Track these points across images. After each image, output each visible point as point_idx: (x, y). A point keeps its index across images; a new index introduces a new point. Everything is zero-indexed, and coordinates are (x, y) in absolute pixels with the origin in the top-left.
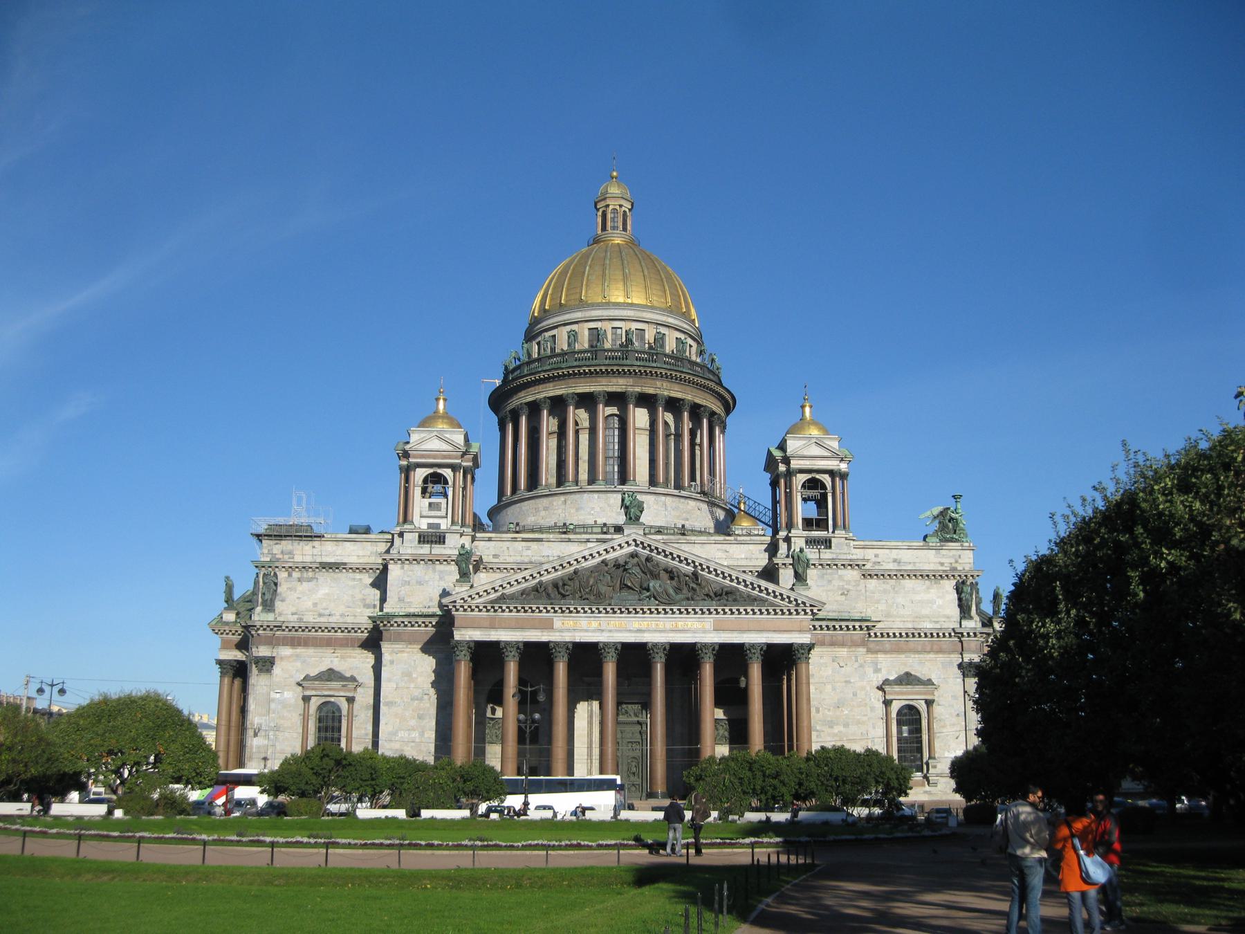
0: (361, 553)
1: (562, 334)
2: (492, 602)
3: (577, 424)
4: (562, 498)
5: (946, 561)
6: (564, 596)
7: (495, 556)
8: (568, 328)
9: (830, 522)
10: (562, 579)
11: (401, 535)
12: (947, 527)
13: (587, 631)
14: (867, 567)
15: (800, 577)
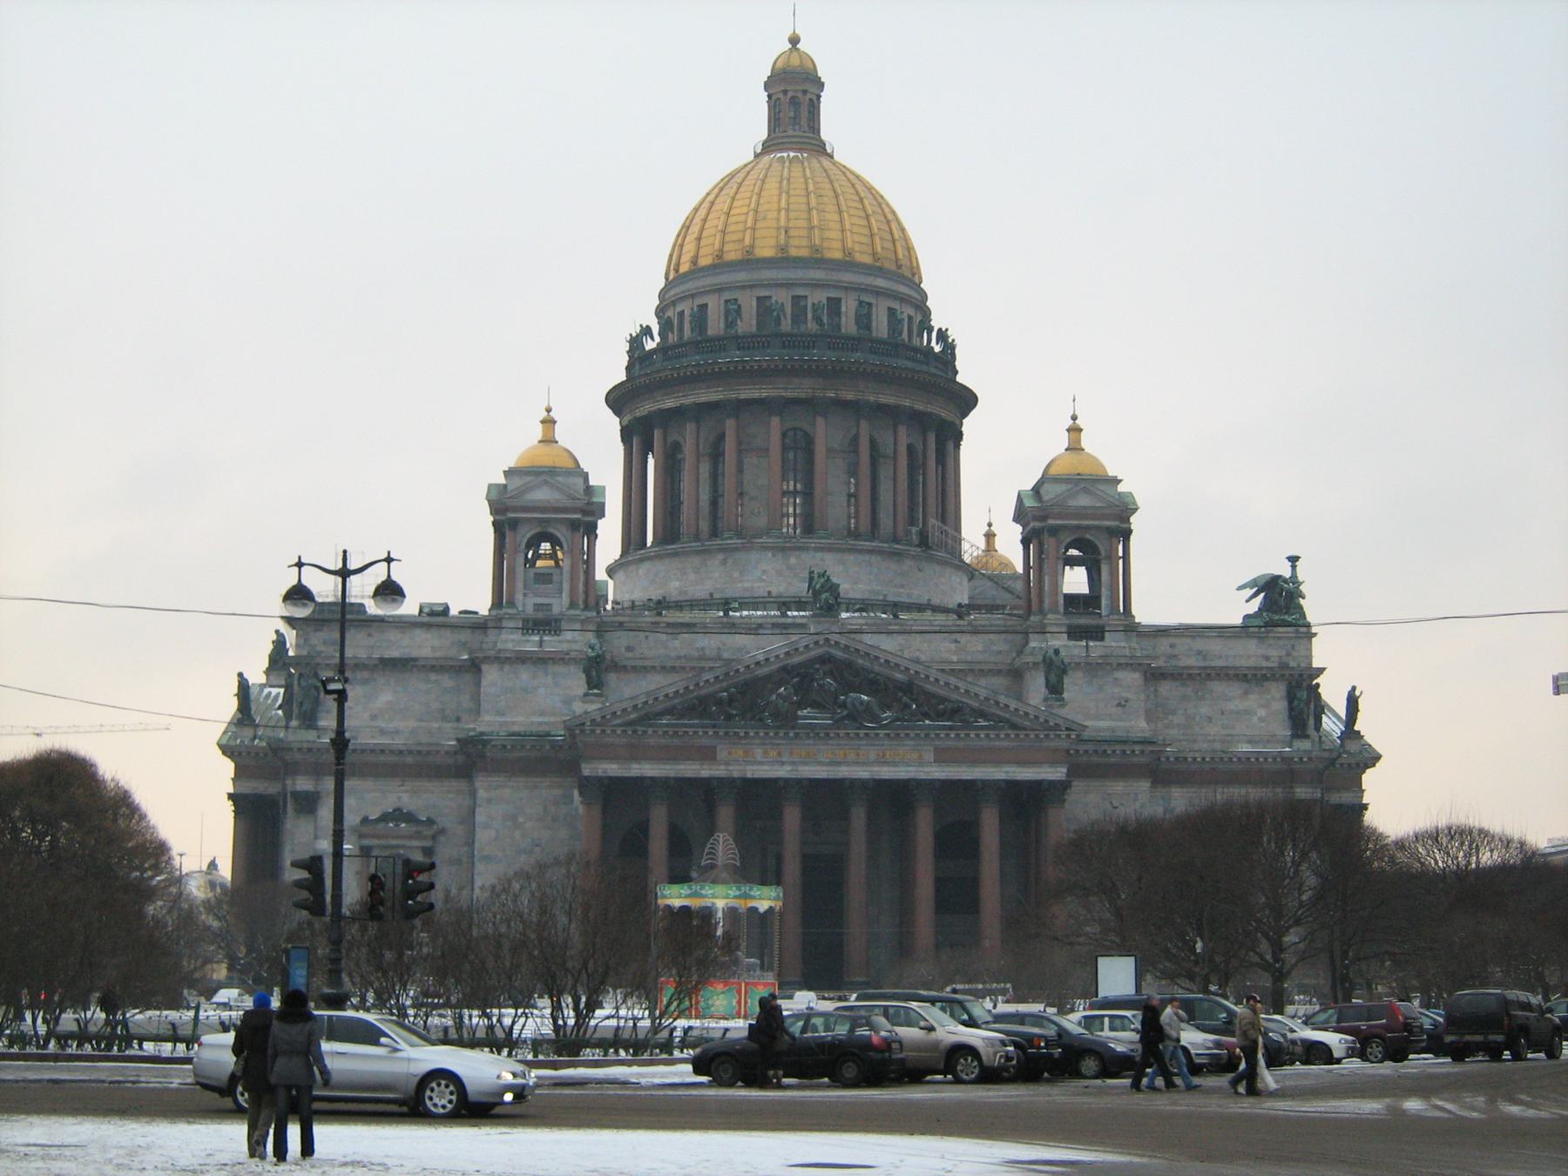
0: (436, 643)
1: (715, 305)
2: (630, 723)
3: (740, 443)
4: (721, 556)
5: (1274, 653)
6: (729, 717)
7: (629, 649)
8: (727, 295)
9: (1104, 602)
10: (726, 690)
11: (500, 620)
12: (1276, 602)
13: (761, 763)
14: (1161, 663)
15: (1055, 689)
